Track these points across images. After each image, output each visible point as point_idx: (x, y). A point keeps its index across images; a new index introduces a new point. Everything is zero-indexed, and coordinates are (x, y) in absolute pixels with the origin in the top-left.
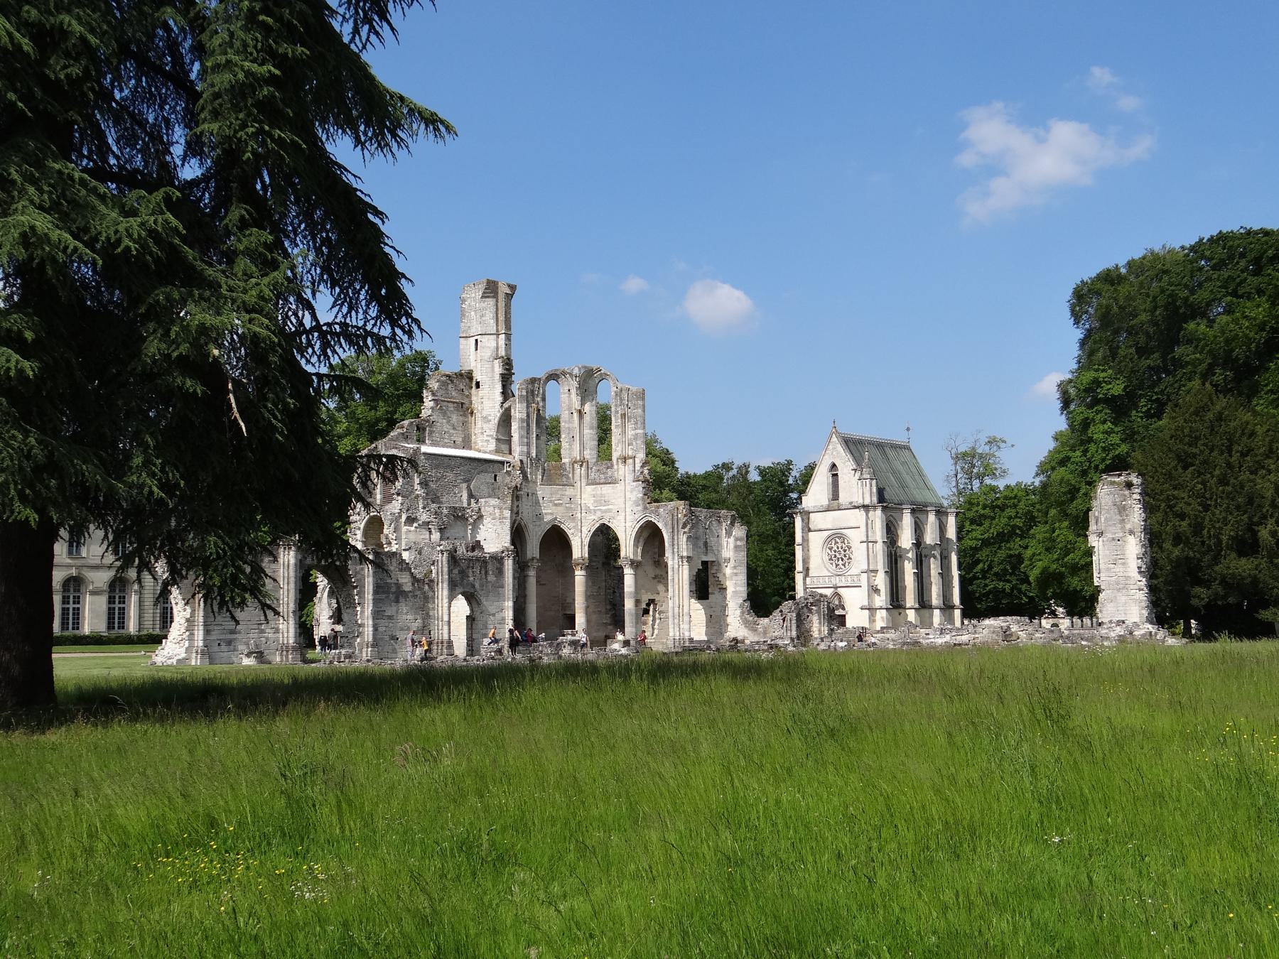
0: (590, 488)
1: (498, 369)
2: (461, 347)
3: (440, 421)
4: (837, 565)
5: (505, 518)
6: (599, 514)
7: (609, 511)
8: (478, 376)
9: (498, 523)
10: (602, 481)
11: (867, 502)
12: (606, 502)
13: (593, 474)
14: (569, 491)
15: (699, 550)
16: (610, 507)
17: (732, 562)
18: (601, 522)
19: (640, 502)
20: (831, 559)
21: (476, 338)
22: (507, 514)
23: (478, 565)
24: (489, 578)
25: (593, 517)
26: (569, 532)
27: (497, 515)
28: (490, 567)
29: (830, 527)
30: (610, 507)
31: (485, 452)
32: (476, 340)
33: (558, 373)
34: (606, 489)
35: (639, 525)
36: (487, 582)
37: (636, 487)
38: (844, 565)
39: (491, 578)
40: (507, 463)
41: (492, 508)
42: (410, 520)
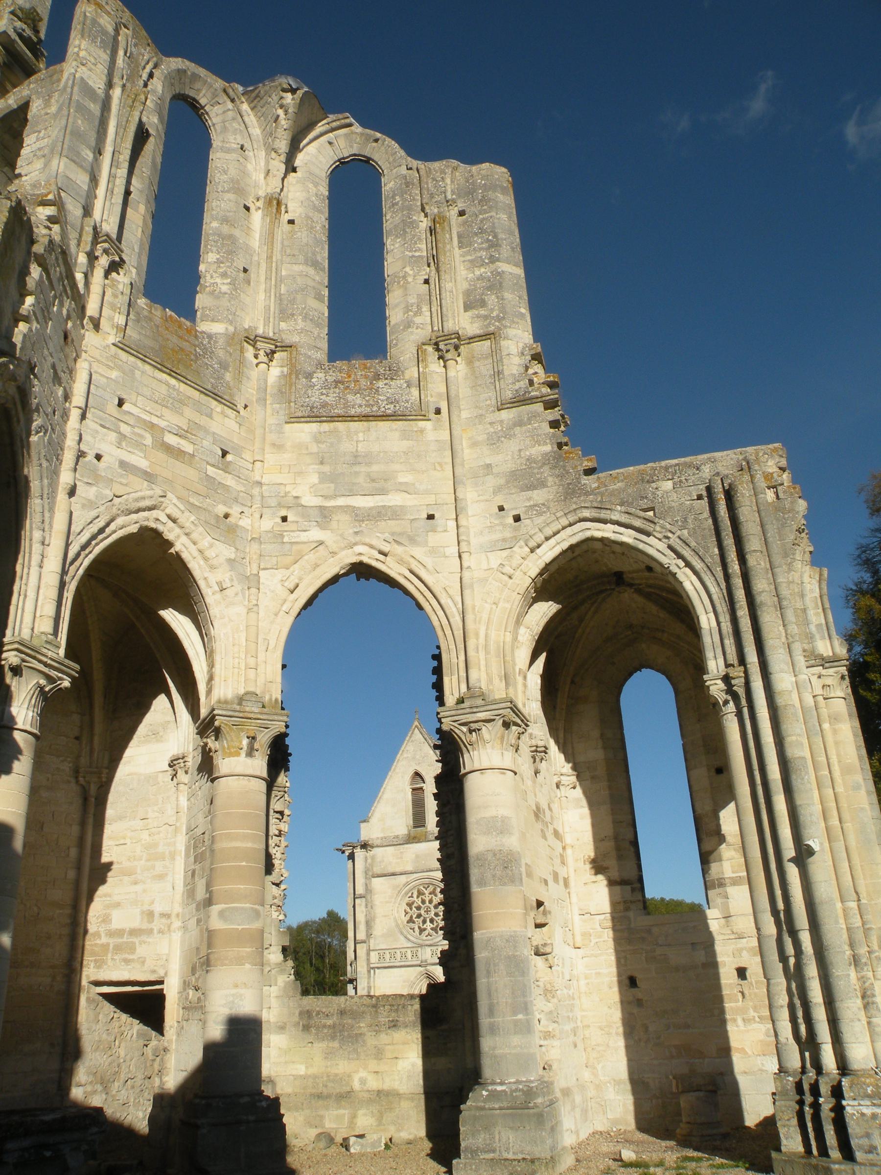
0: (306, 431)
4: (422, 931)
20: (411, 921)
29: (409, 868)
30: (394, 499)
37: (520, 423)
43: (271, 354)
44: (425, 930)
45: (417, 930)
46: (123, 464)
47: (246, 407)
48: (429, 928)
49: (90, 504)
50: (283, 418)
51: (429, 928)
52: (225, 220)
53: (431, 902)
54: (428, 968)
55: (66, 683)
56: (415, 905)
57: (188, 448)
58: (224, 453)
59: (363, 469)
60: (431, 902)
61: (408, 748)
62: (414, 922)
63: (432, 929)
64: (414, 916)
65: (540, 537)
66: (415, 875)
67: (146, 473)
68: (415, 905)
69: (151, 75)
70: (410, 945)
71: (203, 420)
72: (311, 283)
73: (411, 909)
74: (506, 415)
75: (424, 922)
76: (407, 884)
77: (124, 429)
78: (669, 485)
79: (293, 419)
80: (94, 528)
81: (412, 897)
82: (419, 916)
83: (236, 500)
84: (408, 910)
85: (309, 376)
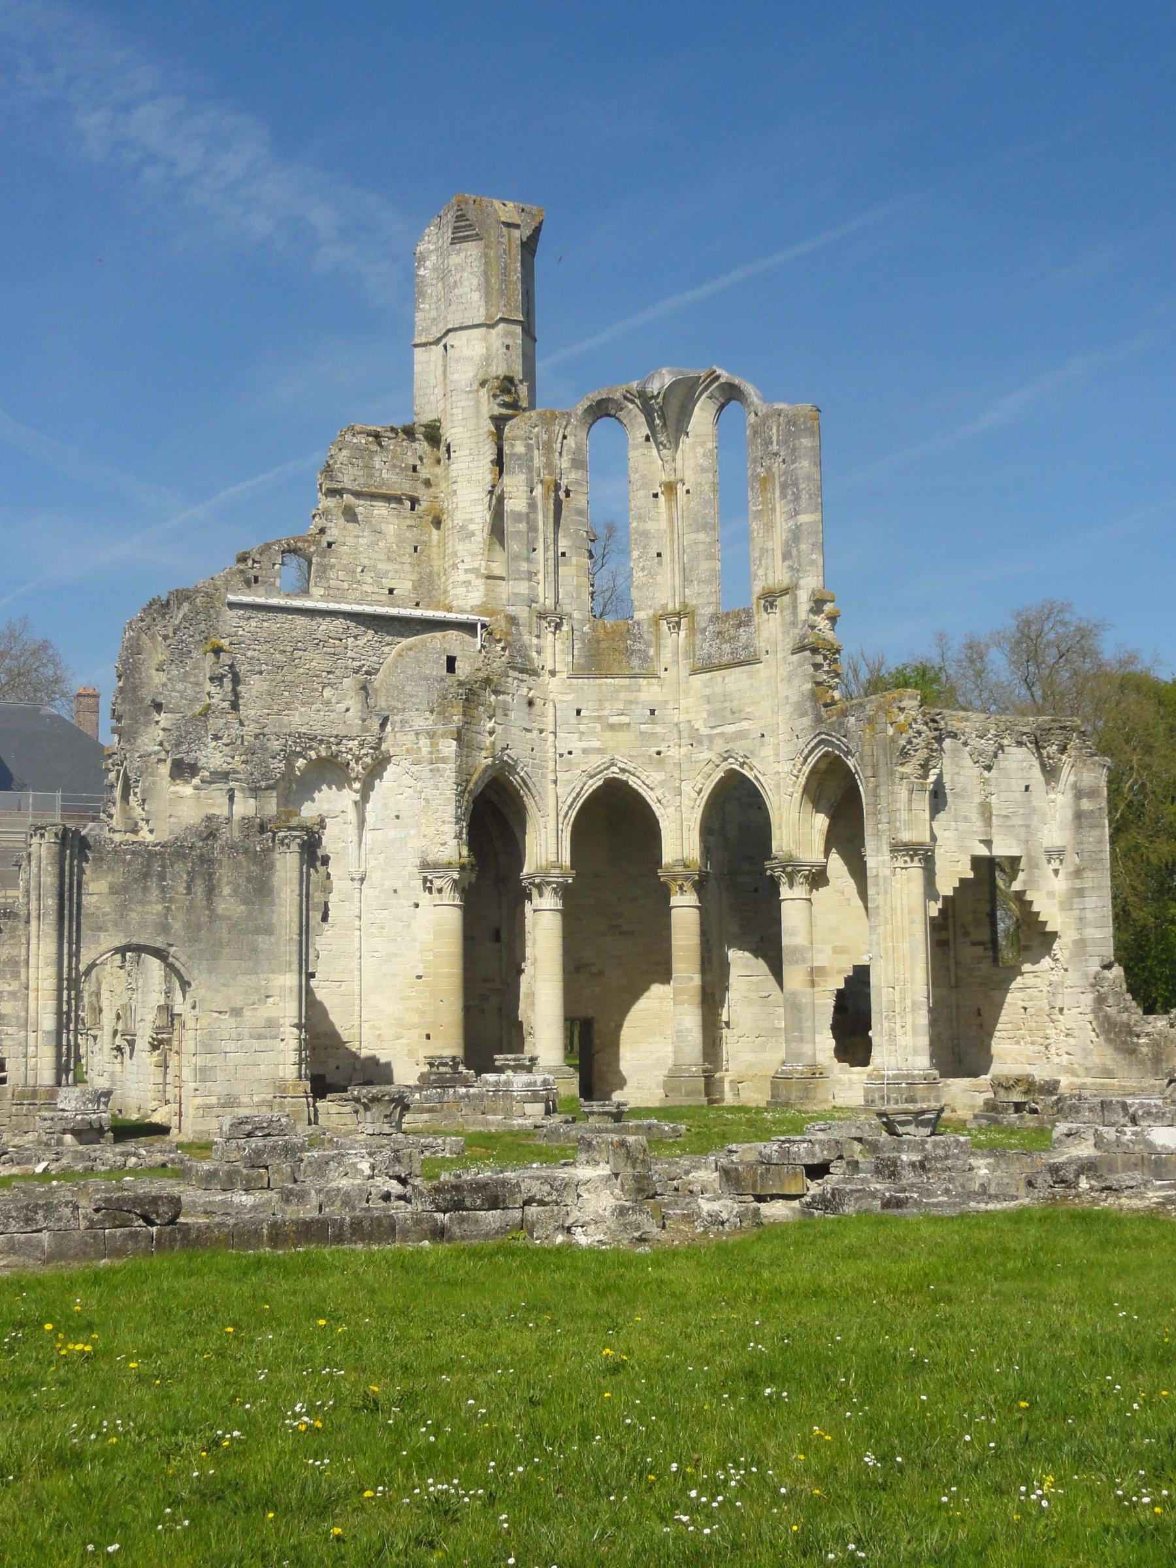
1: (489, 407)
2: (417, 368)
3: (350, 540)
5: (444, 760)
6: (720, 746)
7: (741, 735)
8: (450, 433)
9: (426, 774)
10: (725, 660)
12: (736, 715)
13: (706, 645)
14: (649, 691)
15: (963, 826)
16: (745, 725)
17: (1073, 860)
18: (725, 766)
19: (808, 704)
22: (449, 747)
23: (181, 869)
24: (221, 907)
25: (706, 755)
26: (650, 797)
27: (425, 751)
28: (224, 874)
30: (745, 725)
31: (462, 612)
33: (618, 395)
34: (735, 679)
35: (807, 769)
36: (213, 917)
39: (228, 905)
40: (484, 626)
41: (412, 737)
42: (183, 770)
43: (678, 624)
46: (585, 751)
47: (666, 670)
49: (569, 781)
50: (688, 672)
52: (640, 518)
55: (570, 881)
57: (625, 719)
58: (652, 712)
59: (727, 704)
65: (806, 751)
67: (599, 749)
69: (565, 437)
71: (632, 696)
72: (701, 547)
74: (796, 657)
77: (582, 728)
78: (852, 719)
79: (694, 672)
80: (574, 795)
83: (663, 740)
85: (705, 629)
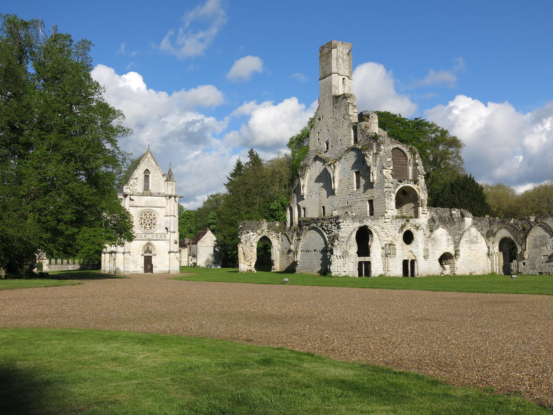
4: (145, 228)
11: (170, 193)
20: (141, 224)
21: (344, 77)
29: (143, 205)
32: (344, 79)
38: (151, 228)
44: (147, 228)
45: (143, 227)
48: (148, 227)
51: (148, 227)
53: (149, 218)
54: (151, 241)
56: (143, 218)
60: (149, 218)
61: (145, 160)
62: (142, 225)
63: (149, 228)
64: (143, 222)
66: (145, 208)
68: (143, 218)
70: (142, 233)
73: (142, 220)
75: (146, 225)
76: (142, 211)
81: (142, 215)
82: (144, 223)
84: (140, 220)
